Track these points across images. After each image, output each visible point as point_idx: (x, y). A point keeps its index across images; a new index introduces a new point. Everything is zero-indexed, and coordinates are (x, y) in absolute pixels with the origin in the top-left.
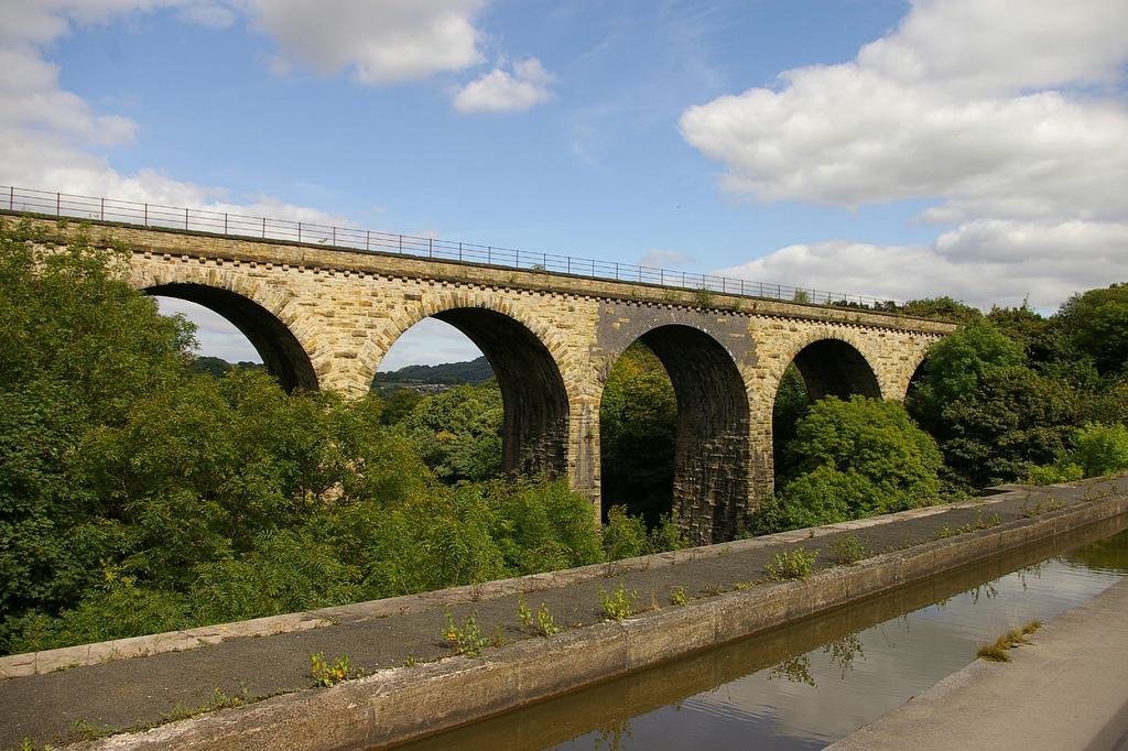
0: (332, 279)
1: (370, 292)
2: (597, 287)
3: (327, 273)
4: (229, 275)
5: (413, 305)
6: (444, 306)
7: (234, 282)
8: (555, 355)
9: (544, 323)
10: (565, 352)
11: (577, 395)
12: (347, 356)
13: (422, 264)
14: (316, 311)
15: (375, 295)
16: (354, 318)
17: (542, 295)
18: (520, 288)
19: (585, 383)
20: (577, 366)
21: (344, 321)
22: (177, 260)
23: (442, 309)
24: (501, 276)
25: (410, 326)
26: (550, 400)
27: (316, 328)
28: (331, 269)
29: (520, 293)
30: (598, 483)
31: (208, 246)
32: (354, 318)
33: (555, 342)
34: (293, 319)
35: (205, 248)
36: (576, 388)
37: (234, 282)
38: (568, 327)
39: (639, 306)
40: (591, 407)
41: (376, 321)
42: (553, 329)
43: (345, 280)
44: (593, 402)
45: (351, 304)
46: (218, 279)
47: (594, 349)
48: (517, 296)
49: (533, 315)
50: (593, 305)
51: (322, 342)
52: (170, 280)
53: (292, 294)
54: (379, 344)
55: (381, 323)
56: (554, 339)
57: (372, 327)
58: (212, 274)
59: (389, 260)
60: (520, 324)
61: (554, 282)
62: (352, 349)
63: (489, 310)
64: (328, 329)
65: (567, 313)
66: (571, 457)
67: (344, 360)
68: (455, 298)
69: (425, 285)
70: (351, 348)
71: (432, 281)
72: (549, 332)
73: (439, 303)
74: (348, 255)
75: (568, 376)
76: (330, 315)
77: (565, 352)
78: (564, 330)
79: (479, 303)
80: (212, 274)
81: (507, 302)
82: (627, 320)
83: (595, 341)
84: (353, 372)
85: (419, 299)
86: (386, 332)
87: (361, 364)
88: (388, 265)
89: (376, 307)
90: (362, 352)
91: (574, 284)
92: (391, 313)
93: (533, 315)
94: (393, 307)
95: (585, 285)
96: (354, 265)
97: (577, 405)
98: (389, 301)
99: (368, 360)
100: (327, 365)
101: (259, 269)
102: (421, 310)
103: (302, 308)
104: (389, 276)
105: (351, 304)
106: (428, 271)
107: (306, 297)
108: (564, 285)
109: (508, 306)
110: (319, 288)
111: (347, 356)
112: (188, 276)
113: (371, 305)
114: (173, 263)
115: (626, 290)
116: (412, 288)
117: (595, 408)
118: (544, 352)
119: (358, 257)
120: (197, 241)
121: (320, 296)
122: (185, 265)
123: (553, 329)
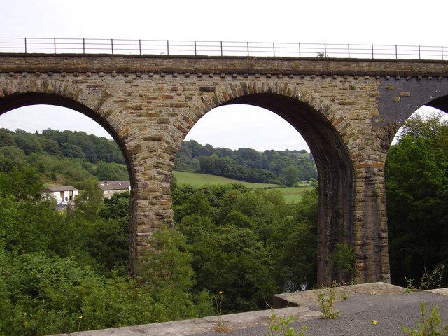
0: (139, 81)
1: (170, 87)
2: (375, 68)
3: (134, 76)
4: (58, 84)
5: (206, 96)
6: (235, 95)
7: (62, 89)
8: (339, 127)
9: (327, 102)
10: (348, 125)
11: (362, 160)
13: (215, 62)
14: (128, 105)
15: (175, 90)
16: (158, 109)
17: (324, 78)
18: (302, 74)
19: (368, 150)
20: (360, 136)
21: (150, 112)
22: (18, 76)
24: (284, 66)
25: (206, 112)
26: (343, 166)
27: (128, 119)
28: (138, 73)
29: (302, 78)
30: (385, 235)
31: (42, 64)
32: (158, 109)
33: (337, 117)
34: (109, 114)
35: (39, 66)
36: (359, 155)
37: (62, 89)
38: (350, 104)
40: (376, 170)
41: (176, 111)
42: (335, 107)
43: (150, 80)
44: (377, 166)
45: (156, 99)
46: (50, 88)
47: (377, 121)
48: (300, 81)
49: (316, 95)
50: (373, 84)
51: (134, 129)
52: (14, 90)
53: (107, 94)
54: (180, 128)
55: (181, 112)
56: (337, 114)
57: (173, 115)
58: (46, 84)
59: (186, 62)
60: (305, 104)
61: (333, 67)
63: (275, 94)
64: (138, 119)
65: (349, 92)
66: (359, 213)
67: (151, 142)
68: (244, 86)
69: (217, 79)
70: (157, 133)
71: (223, 75)
74: (152, 61)
75: (352, 145)
76: (138, 108)
77: (348, 125)
78: (346, 107)
79: (266, 89)
80: (46, 84)
81: (291, 87)
83: (377, 113)
84: (160, 151)
86: (185, 119)
87: (165, 144)
88: (184, 66)
89: (175, 101)
90: (166, 136)
92: (190, 103)
93: (316, 95)
94: (190, 99)
95: (365, 66)
96: (156, 67)
97: (362, 170)
98: (187, 93)
99: (171, 142)
100: (138, 148)
101: (80, 78)
102: (215, 99)
103: (116, 105)
104: (186, 74)
105: (156, 99)
106: (220, 67)
107: (119, 96)
108: (344, 68)
109: (292, 90)
110: (129, 88)
112: (28, 87)
113: (172, 98)
114: (16, 78)
116: (207, 82)
117: (379, 170)
118: (329, 125)
119: (159, 62)
120: (34, 61)
122: (23, 80)
123: (335, 107)
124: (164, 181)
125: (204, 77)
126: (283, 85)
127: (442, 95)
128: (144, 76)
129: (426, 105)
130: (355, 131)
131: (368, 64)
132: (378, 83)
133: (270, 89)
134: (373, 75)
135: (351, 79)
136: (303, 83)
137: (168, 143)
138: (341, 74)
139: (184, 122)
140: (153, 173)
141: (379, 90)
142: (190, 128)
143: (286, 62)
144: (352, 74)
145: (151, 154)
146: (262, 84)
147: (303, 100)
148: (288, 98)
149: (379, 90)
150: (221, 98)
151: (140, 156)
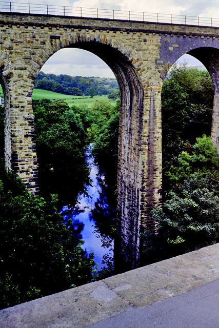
0: (10, 30)
1: (31, 35)
2: (159, 28)
8: (136, 65)
9: (130, 49)
12: (21, 69)
18: (115, 30)
19: (153, 80)
23: (71, 43)
25: (54, 52)
28: (11, 24)
29: (115, 32)
33: (136, 58)
36: (147, 83)
39: (184, 37)
41: (35, 51)
42: (134, 51)
50: (157, 39)
54: (38, 63)
56: (134, 56)
57: (33, 54)
62: (23, 66)
65: (142, 43)
67: (20, 71)
69: (61, 29)
72: (132, 53)
73: (69, 39)
76: (10, 48)
77: (142, 63)
79: (92, 39)
82: (177, 46)
83: (159, 57)
84: (25, 77)
85: (59, 38)
89: (36, 44)
91: (147, 27)
93: (123, 44)
95: (153, 27)
102: (60, 44)
104: (42, 26)
105: (22, 42)
111: (21, 69)
113: (32, 43)
115: (176, 29)
116: (56, 32)
121: (5, 39)
123: (134, 51)
124: (27, 96)
125: (54, 29)
126: (103, 37)
127: (197, 47)
128: (14, 27)
129: (187, 53)
130: (146, 68)
131: (155, 26)
132: (160, 37)
133: (95, 39)
134: (158, 32)
135: (144, 34)
136: (115, 36)
137: (30, 72)
138: (139, 31)
139: (40, 58)
140: (21, 91)
141: (161, 42)
142: (44, 62)
143: (105, 22)
144: (144, 31)
145: (19, 79)
146: (90, 35)
147: (115, 47)
148: (106, 45)
149: (161, 42)
150: (64, 43)
151: (12, 80)
